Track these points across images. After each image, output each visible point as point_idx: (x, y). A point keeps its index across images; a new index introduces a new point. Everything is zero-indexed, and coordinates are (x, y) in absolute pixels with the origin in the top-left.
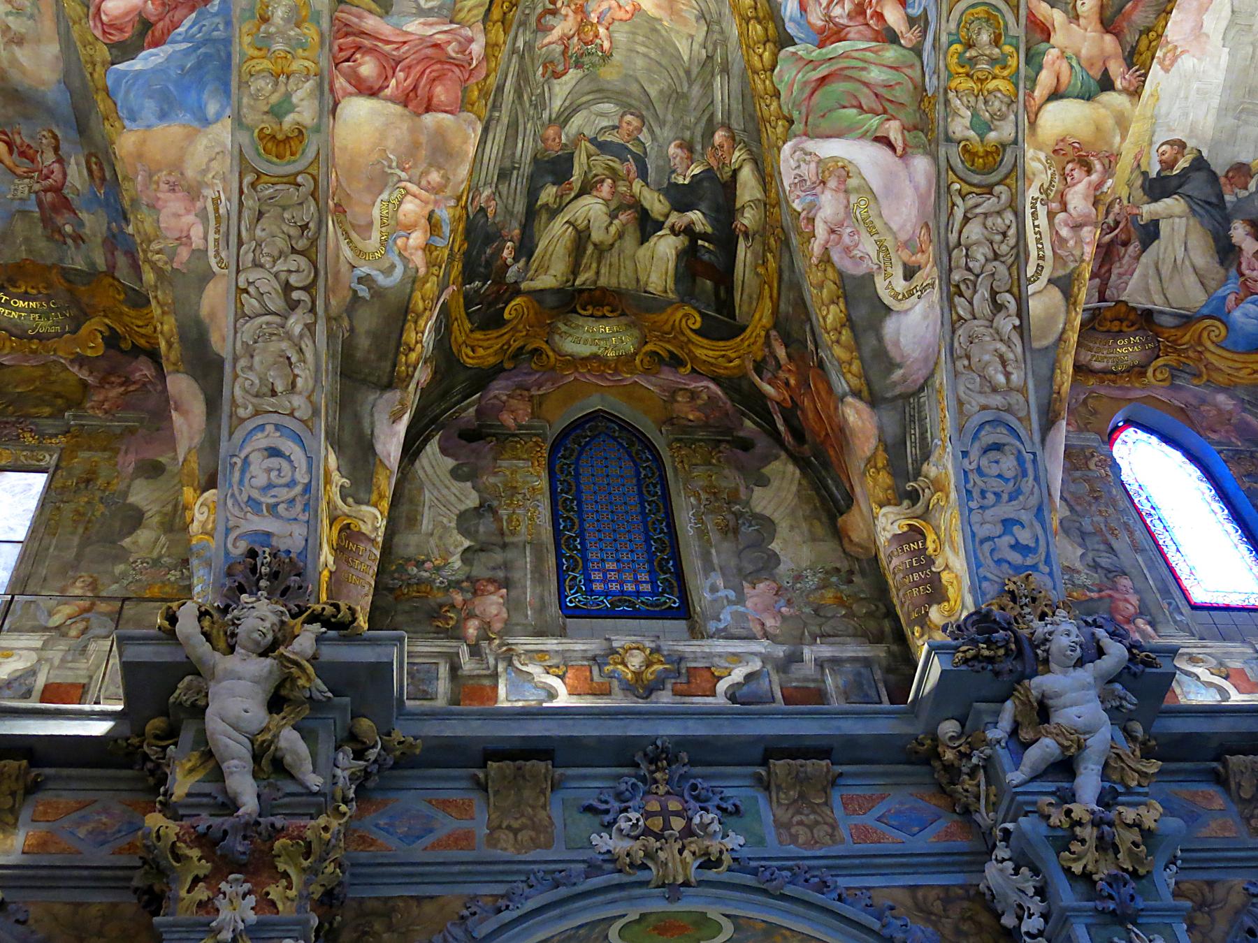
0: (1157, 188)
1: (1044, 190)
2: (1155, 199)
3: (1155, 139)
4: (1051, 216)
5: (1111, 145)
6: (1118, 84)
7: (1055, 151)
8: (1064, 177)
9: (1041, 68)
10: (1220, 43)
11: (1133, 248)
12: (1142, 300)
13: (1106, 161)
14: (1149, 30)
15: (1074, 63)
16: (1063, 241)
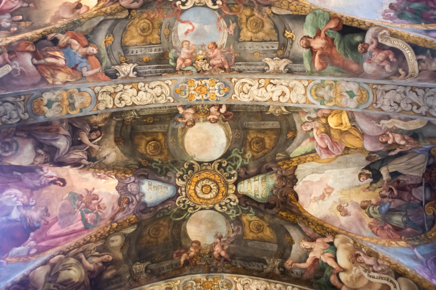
0: (376, 177)
1: (366, 271)
2: (381, 176)
3: (357, 185)
4: (374, 271)
5: (351, 247)
6: (331, 240)
7: (353, 263)
8: (361, 263)
9: (326, 264)
10: (323, 174)
11: (401, 178)
12: (422, 170)
13: (356, 249)
14: (314, 230)
15: (325, 251)
16: (382, 270)
